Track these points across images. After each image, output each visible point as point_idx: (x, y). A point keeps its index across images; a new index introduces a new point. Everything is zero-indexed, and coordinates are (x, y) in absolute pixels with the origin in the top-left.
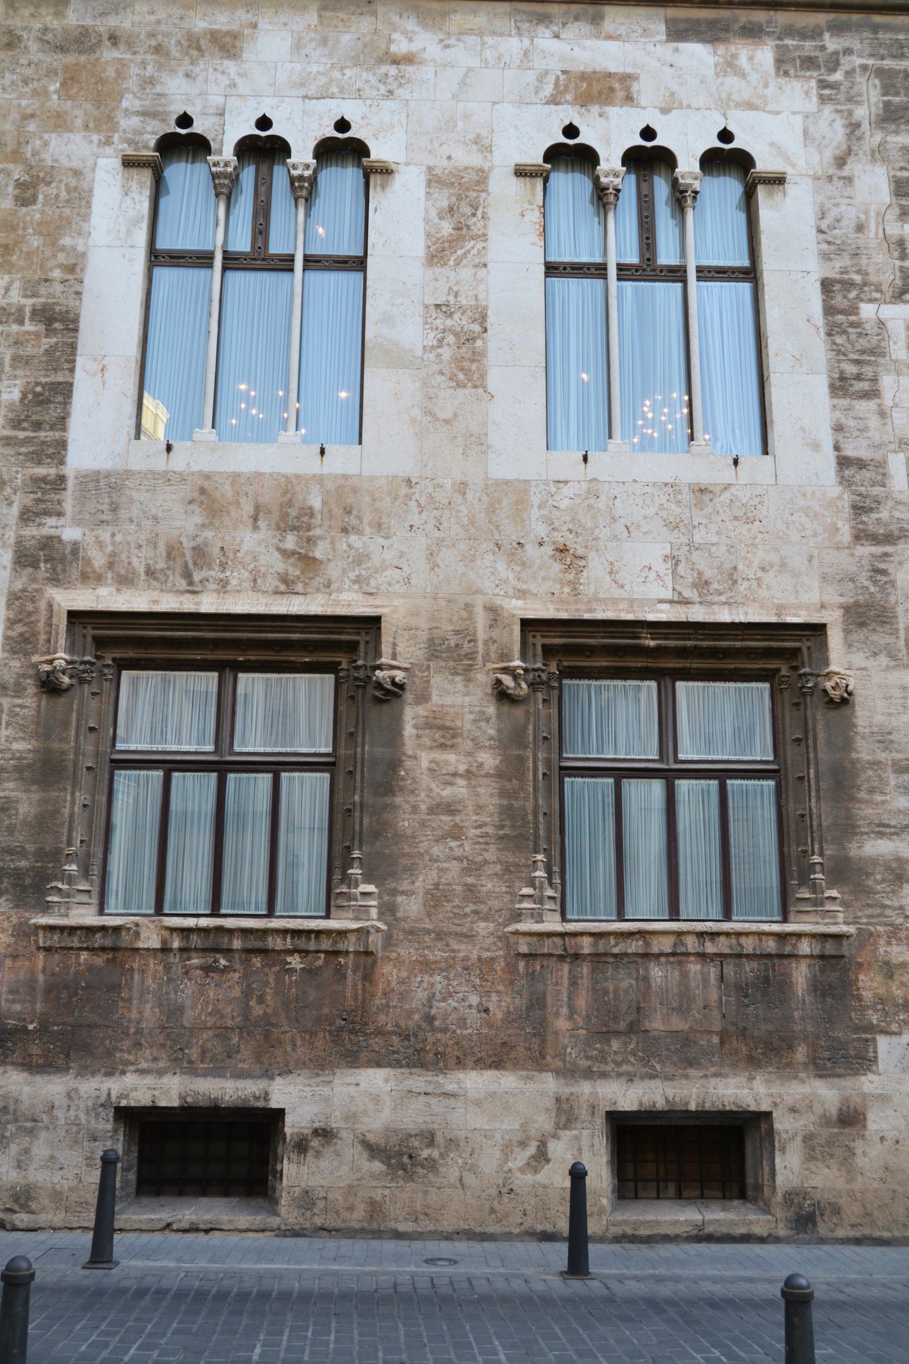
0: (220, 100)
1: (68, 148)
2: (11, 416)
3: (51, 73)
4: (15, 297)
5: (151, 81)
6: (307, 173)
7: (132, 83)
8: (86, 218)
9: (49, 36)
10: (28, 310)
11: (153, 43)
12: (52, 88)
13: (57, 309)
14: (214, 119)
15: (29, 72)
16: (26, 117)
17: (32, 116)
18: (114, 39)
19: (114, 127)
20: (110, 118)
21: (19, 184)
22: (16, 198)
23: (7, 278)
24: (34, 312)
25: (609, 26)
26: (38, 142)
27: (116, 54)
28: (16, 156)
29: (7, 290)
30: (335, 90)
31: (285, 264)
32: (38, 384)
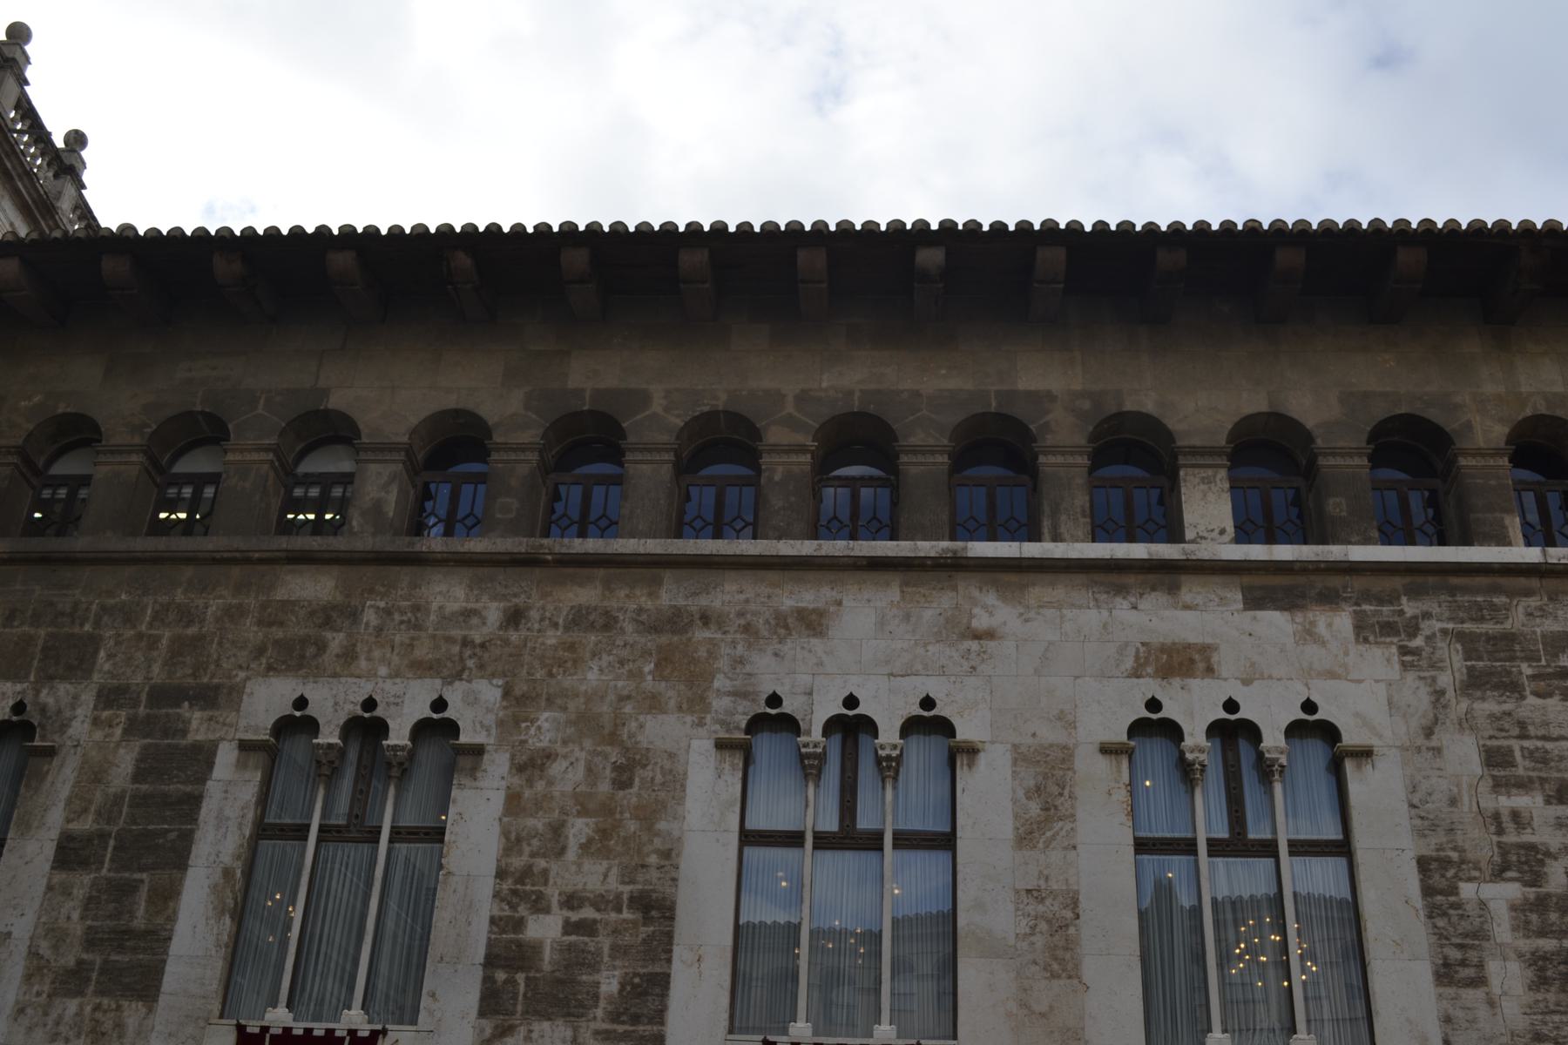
0: (807, 679)
1: (661, 731)
2: (610, 1008)
3: (646, 653)
4: (613, 884)
5: (741, 661)
6: (895, 753)
7: (723, 663)
8: (681, 801)
9: (644, 617)
10: (625, 897)
11: (742, 622)
12: (647, 669)
13: (654, 896)
14: (803, 698)
15: (625, 653)
16: (623, 699)
17: (629, 697)
18: (705, 619)
19: (707, 708)
20: (703, 699)
21: (617, 768)
22: (614, 782)
23: (605, 864)
24: (632, 899)
25: (1186, 595)
26: (634, 724)
27: (707, 634)
28: (613, 738)
29: (606, 876)
30: (920, 667)
31: (873, 842)
32: (636, 975)
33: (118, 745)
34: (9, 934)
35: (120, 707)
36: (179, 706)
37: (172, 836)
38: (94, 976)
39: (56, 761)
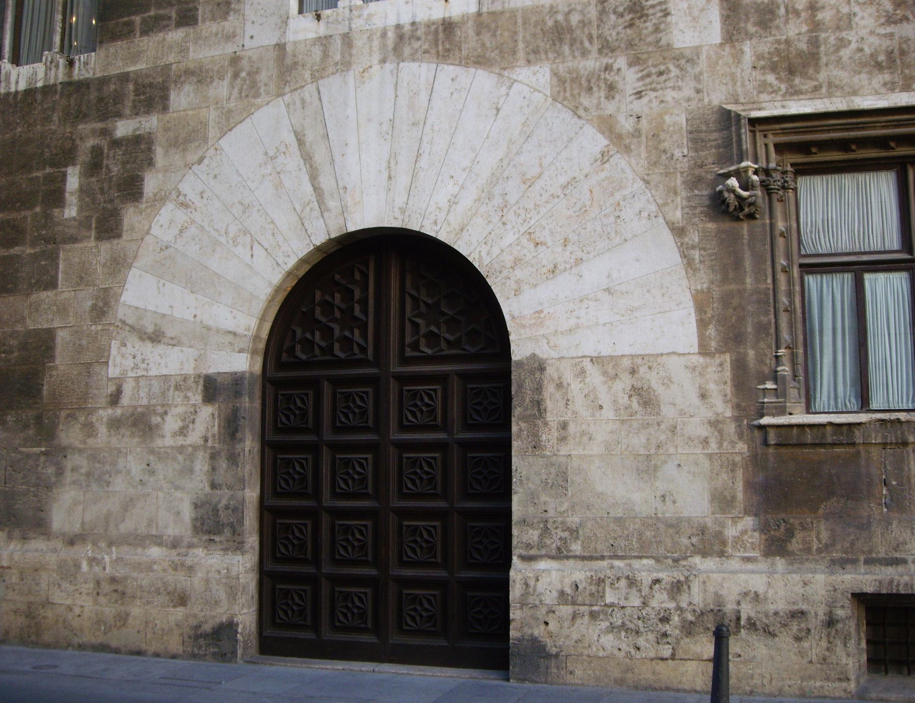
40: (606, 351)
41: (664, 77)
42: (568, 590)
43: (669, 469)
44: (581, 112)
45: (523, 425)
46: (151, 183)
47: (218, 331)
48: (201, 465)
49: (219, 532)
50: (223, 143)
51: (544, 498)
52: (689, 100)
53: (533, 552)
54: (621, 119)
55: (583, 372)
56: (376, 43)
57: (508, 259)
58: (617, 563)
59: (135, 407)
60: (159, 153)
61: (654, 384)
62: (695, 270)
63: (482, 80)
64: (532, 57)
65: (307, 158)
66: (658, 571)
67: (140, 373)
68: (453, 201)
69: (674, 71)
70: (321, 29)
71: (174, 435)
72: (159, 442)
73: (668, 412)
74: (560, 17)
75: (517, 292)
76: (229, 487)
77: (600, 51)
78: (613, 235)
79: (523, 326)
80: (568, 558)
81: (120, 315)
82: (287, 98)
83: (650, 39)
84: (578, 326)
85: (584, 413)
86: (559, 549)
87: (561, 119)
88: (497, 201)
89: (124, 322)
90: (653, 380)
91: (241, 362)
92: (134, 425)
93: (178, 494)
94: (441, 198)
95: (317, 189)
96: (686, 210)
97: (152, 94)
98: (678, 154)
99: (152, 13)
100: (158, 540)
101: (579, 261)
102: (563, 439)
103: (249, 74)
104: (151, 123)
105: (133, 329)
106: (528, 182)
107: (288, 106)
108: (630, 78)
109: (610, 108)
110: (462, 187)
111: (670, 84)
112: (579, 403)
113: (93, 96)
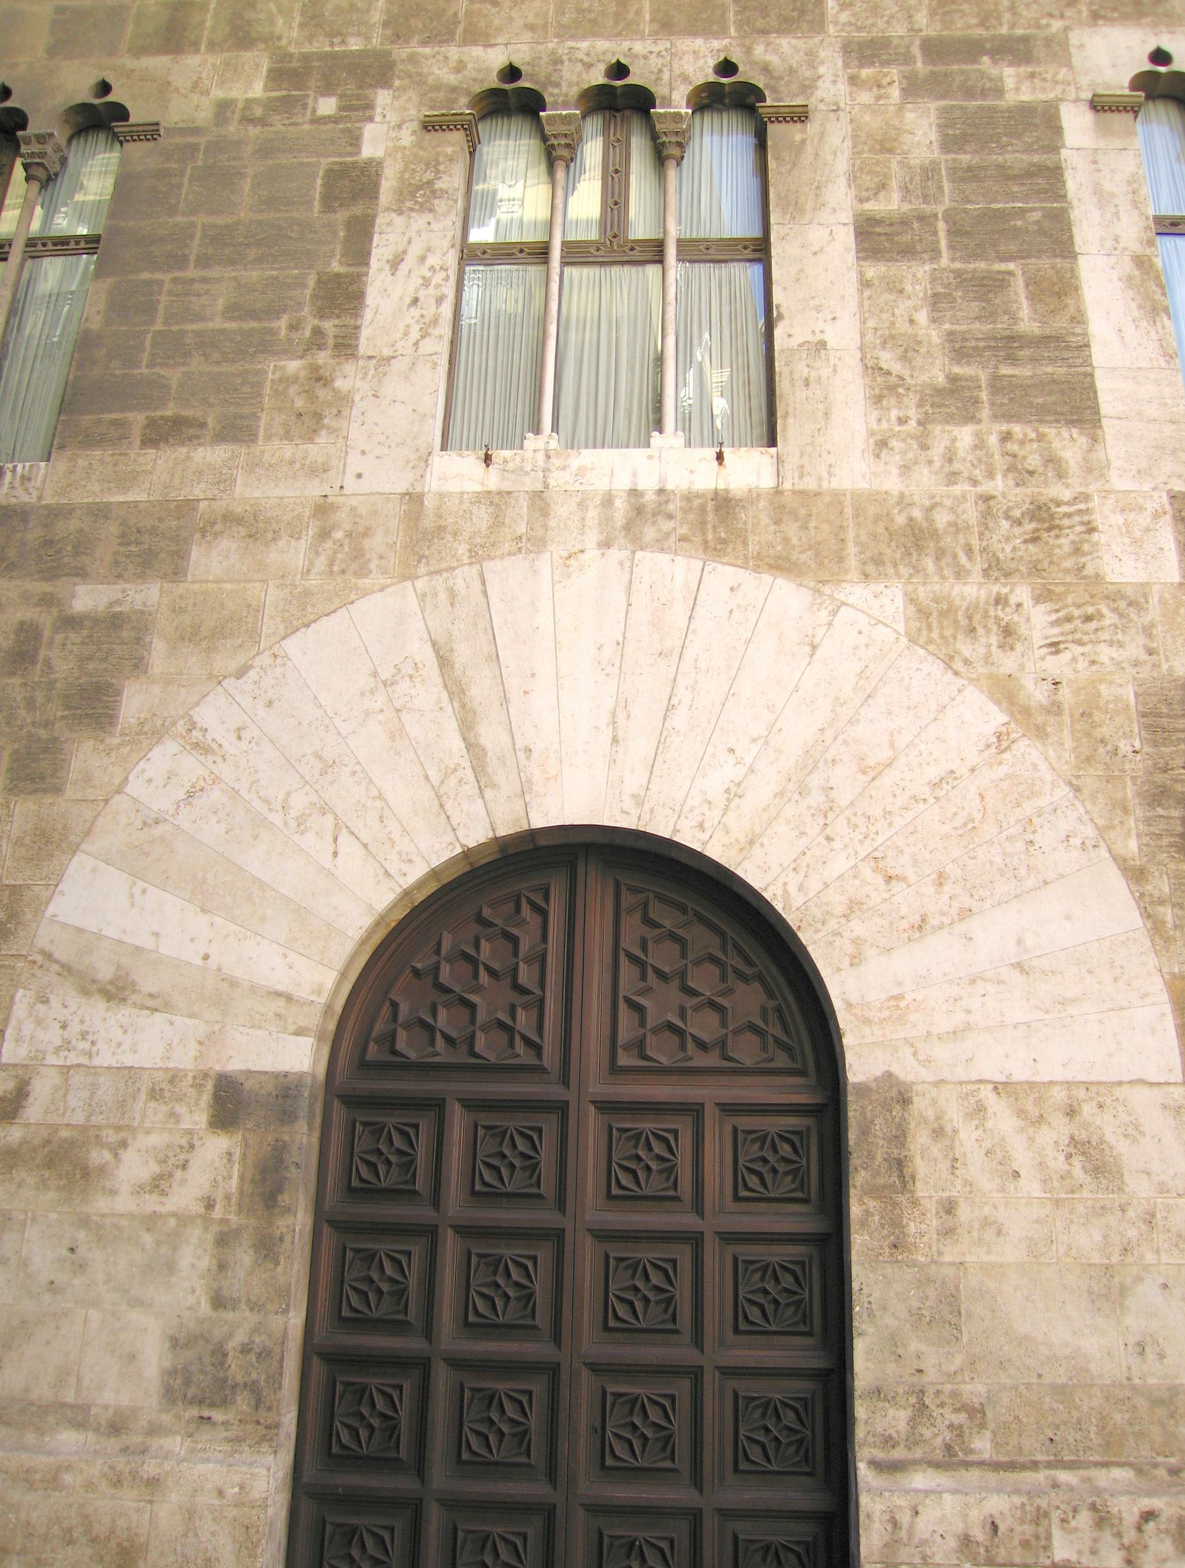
33: (900, 109)
34: (822, 344)
35: (887, 63)
36: (974, 61)
37: (1036, 216)
38: (984, 395)
39: (811, 128)
40: (1020, 1074)
41: (1094, 625)
42: (979, 1534)
43: (1148, 1291)
44: (958, 665)
45: (872, 1204)
46: (134, 702)
47: (253, 989)
48: (194, 1256)
49: (224, 1403)
50: (291, 646)
51: (914, 1346)
52: (1136, 664)
53: (898, 1454)
54: (1028, 683)
55: (980, 1109)
56: (593, 514)
57: (837, 901)
58: (1063, 1476)
59: (56, 1128)
60: (158, 649)
61: (1110, 1137)
62: (1168, 940)
63: (786, 597)
64: (871, 569)
65: (456, 690)
66: (1149, 1493)
67: (73, 1059)
68: (734, 793)
69: (1110, 618)
70: (493, 479)
71: (139, 1190)
72: (101, 1204)
73: (1139, 1188)
74: (917, 513)
75: (856, 960)
76: (253, 1306)
77: (986, 573)
78: (1023, 872)
79: (867, 1021)
80: (967, 1465)
81: (42, 941)
82: (421, 584)
83: (1068, 564)
84: (968, 1027)
85: (987, 1184)
86: (948, 1447)
87: (923, 673)
88: (816, 798)
89: (49, 956)
90: (1109, 1128)
91: (297, 1054)
92: (50, 1164)
93: (135, 1315)
94: (715, 783)
95: (472, 747)
96: (1146, 839)
97: (156, 543)
98: (1124, 747)
99: (169, 413)
100: (78, 1416)
101: (966, 913)
102: (948, 1232)
103: (349, 535)
104: (147, 595)
105: (67, 969)
106: (871, 772)
107: (422, 597)
108: (1038, 621)
109: (1008, 663)
110: (752, 770)
111: (1104, 636)
112: (976, 1166)
113: (34, 535)
